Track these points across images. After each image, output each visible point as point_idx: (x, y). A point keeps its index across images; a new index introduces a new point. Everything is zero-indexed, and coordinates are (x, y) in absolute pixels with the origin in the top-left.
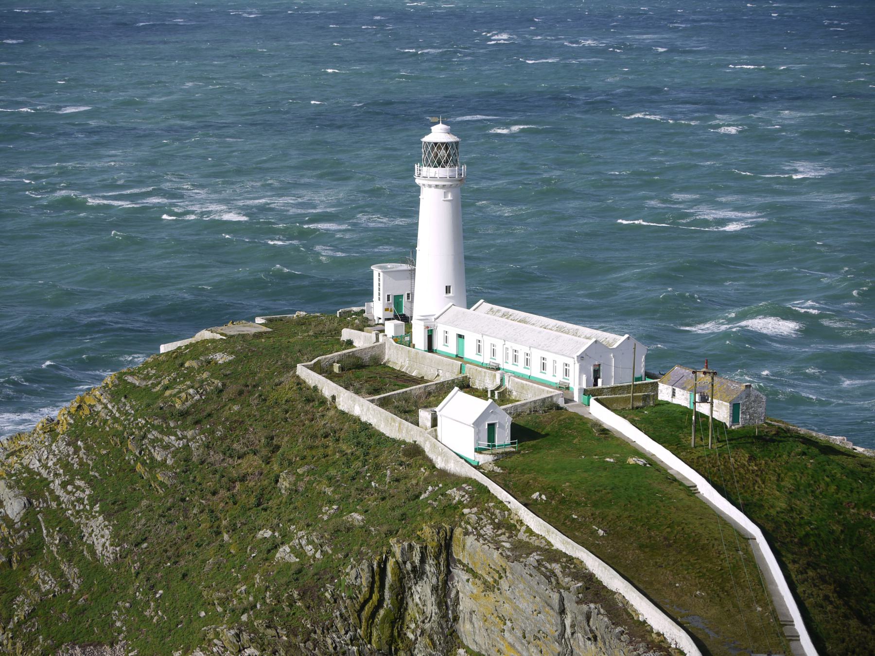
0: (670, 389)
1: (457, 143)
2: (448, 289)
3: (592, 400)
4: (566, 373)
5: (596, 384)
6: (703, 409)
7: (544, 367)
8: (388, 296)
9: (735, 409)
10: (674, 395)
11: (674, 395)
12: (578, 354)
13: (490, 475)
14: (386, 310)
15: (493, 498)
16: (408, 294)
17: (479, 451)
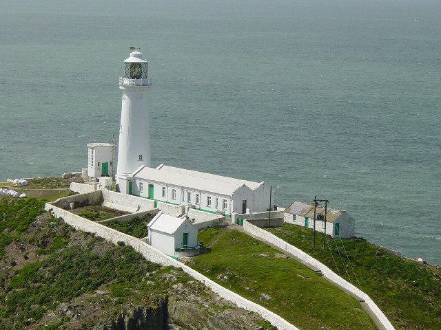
3: (244, 221)
4: (224, 206)
5: (244, 211)
6: (319, 226)
7: (209, 202)
9: (337, 226)
10: (294, 218)
11: (294, 218)
13: (187, 264)
15: (192, 279)
17: (177, 250)
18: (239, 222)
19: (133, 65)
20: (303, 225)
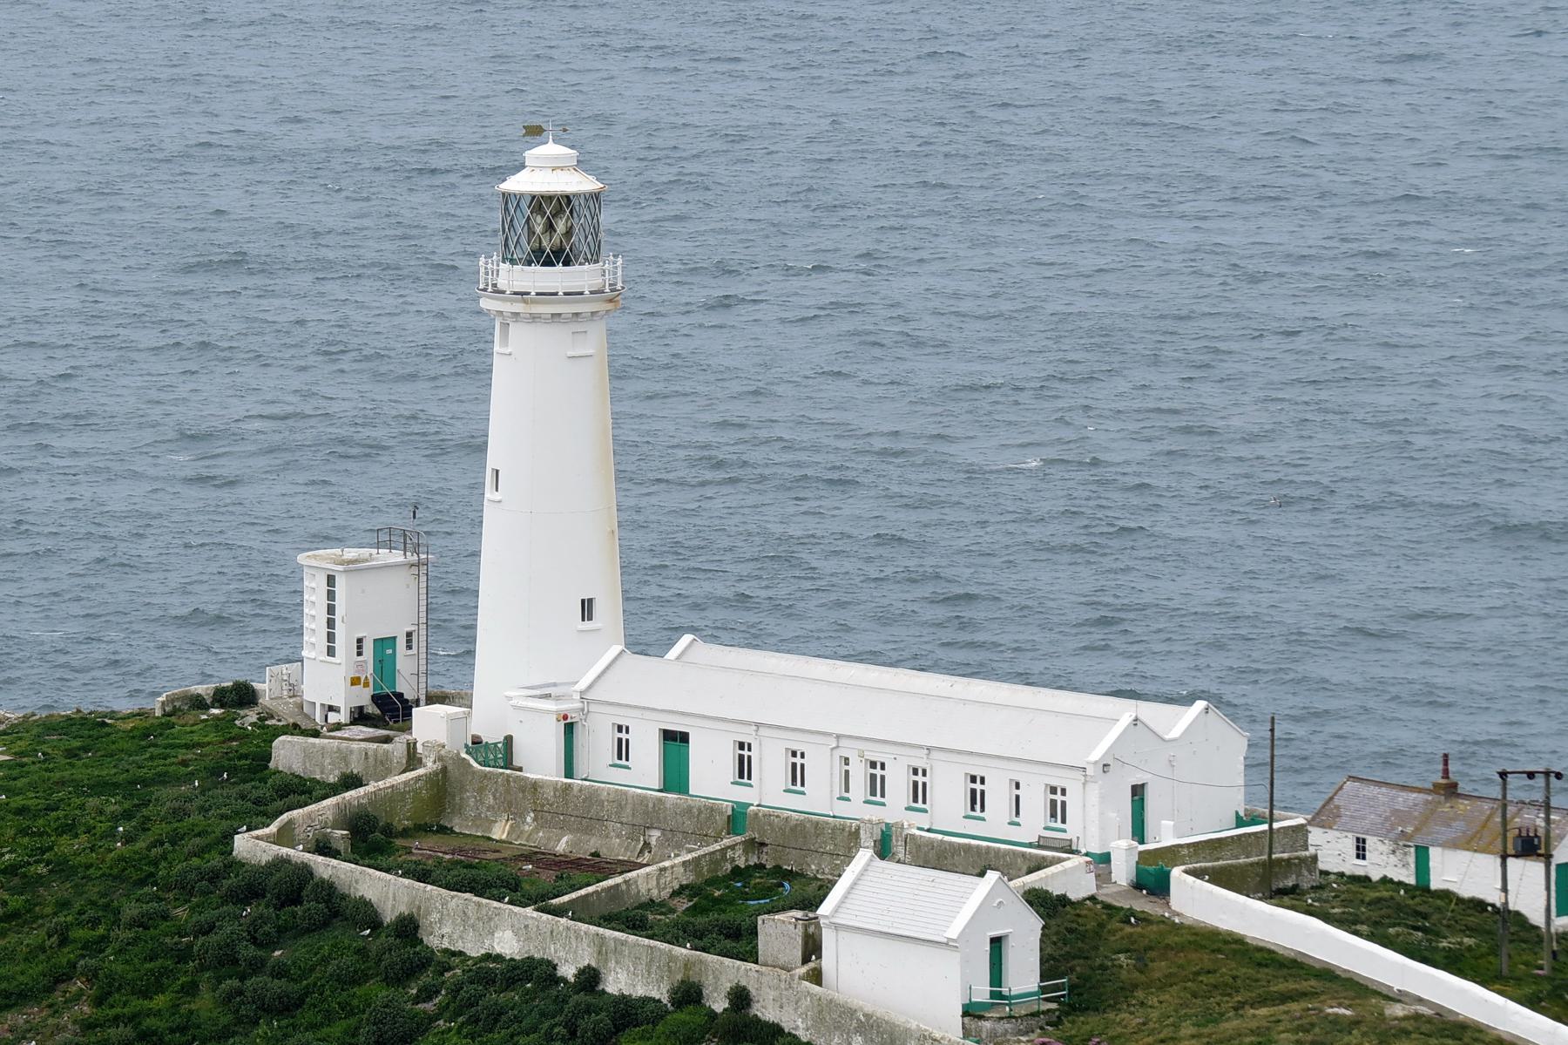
0: (1349, 845)
1: (596, 196)
2: (587, 608)
3: (1177, 873)
4: (1057, 811)
7: (976, 800)
8: (360, 641)
10: (1361, 852)
11: (1361, 852)
12: (1096, 755)
14: (355, 681)
16: (409, 634)
18: (1152, 880)
19: (539, 203)
20: (1412, 881)
